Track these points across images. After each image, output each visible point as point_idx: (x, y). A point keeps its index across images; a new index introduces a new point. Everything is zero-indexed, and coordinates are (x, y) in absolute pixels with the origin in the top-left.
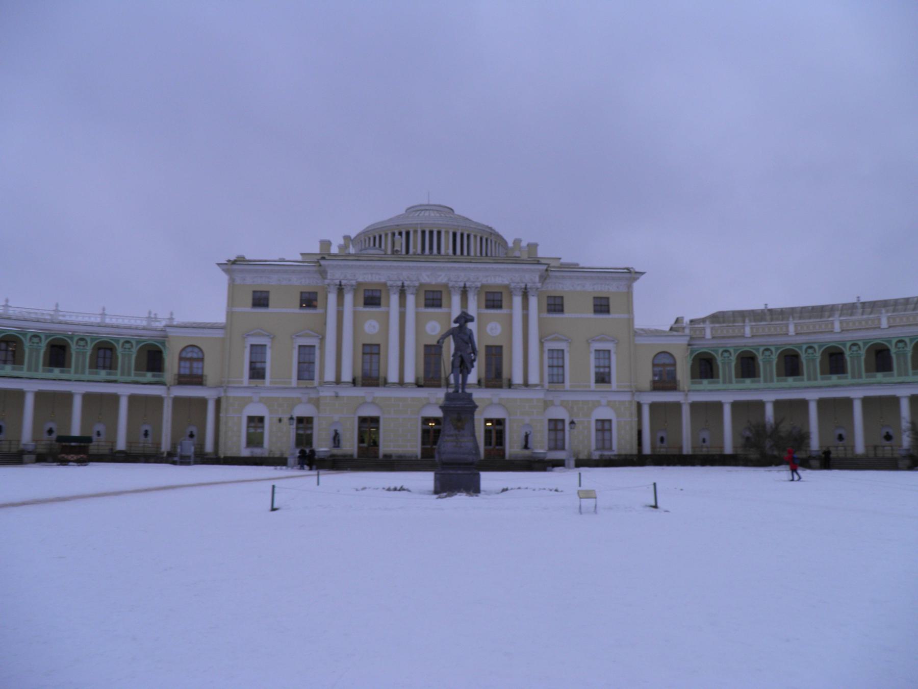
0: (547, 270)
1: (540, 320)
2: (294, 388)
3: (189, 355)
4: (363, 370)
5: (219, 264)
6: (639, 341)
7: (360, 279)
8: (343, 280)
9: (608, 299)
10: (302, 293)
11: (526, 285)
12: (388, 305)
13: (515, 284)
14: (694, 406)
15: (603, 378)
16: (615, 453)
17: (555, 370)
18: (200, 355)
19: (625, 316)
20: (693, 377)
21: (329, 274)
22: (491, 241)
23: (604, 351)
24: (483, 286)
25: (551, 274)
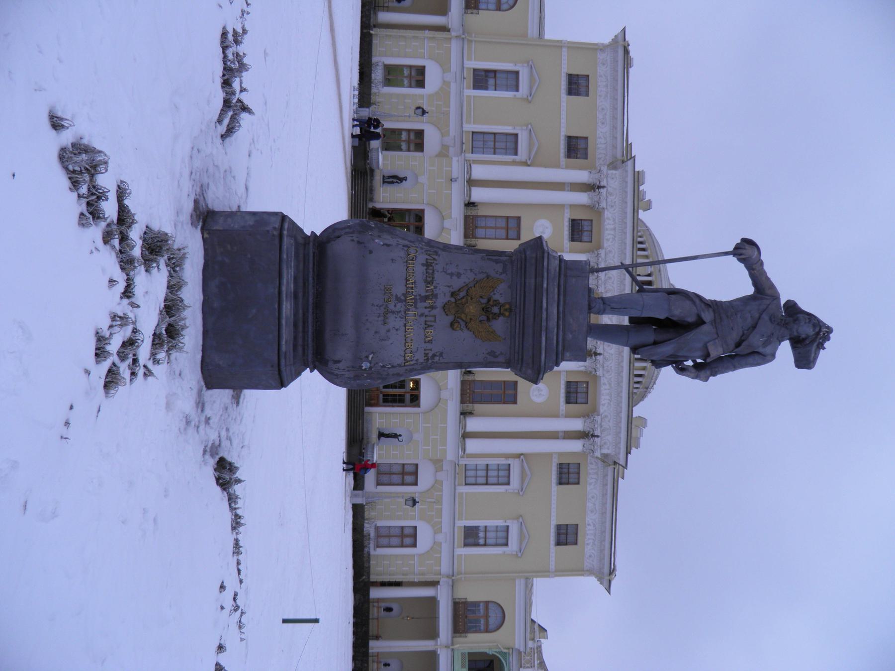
0: (615, 463)
1: (548, 456)
2: (462, 127)
5: (624, 30)
6: (520, 585)
7: (607, 214)
8: (607, 190)
10: (586, 138)
11: (598, 436)
15: (472, 536)
16: (372, 552)
17: (482, 473)
18: (504, 7)
19: (552, 567)
20: (470, 654)
21: (614, 172)
23: (507, 538)
24: (596, 378)
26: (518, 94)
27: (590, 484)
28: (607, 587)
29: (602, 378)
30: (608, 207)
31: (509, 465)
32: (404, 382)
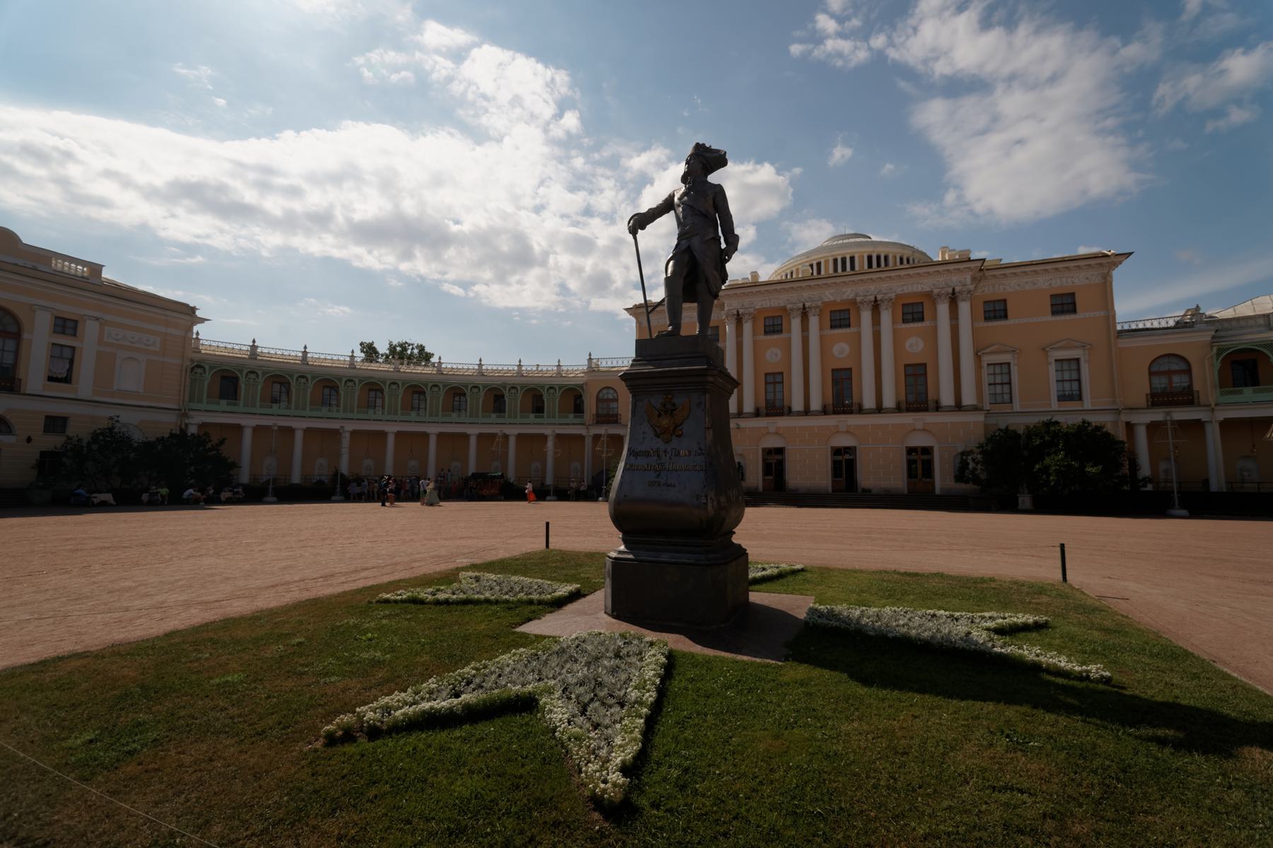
0: (981, 270)
3: (605, 397)
4: (766, 400)
9: (1073, 294)
11: (954, 289)
12: (789, 331)
13: (938, 290)
14: (1226, 425)
19: (1102, 313)
20: (1222, 384)
21: (726, 305)
23: (1069, 360)
24: (898, 297)
25: (988, 273)
27: (1005, 289)
29: (898, 293)
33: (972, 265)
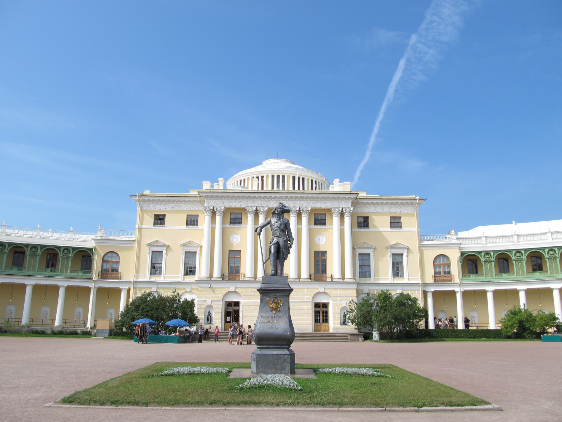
1: (353, 234)
3: (110, 259)
22: (319, 182)
26: (164, 252)
28: (424, 200)
29: (312, 207)
30: (224, 205)
31: (359, 254)
32: (316, 311)
33: (353, 196)
